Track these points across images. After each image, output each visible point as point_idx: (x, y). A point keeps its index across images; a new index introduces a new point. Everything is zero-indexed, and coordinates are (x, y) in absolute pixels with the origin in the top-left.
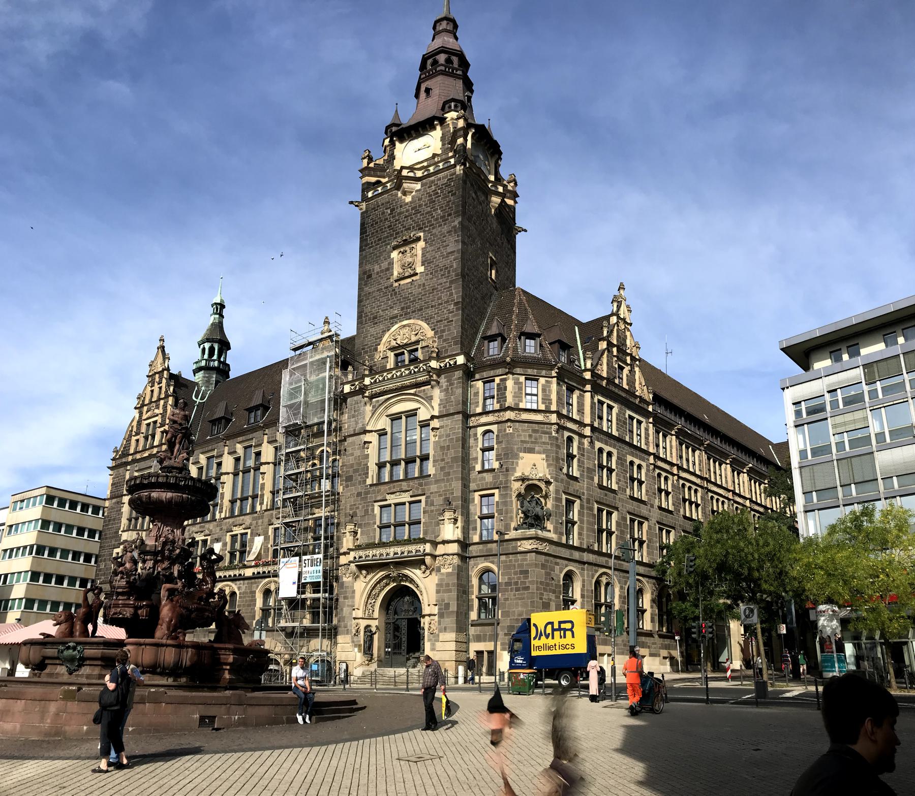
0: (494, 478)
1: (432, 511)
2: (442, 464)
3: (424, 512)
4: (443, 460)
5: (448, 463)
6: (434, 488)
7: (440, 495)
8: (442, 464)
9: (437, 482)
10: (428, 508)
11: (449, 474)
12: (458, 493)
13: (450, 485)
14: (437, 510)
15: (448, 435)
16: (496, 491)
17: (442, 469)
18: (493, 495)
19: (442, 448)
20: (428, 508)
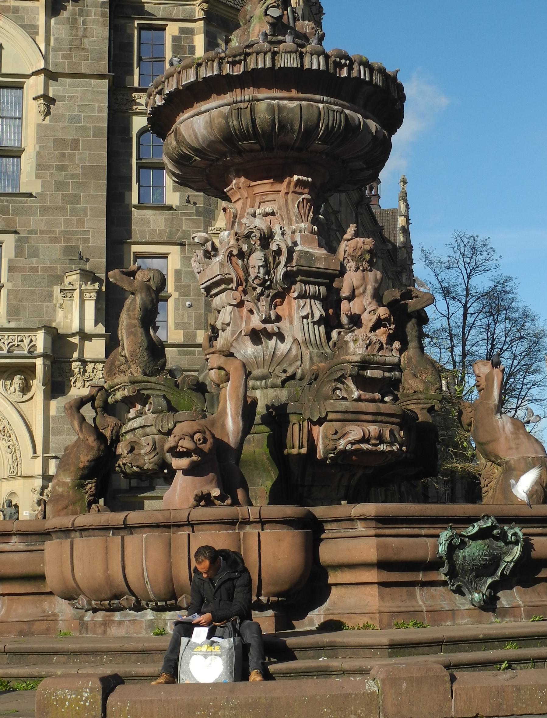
0: (170, 222)
1: (34, 270)
2: (61, 176)
3: (11, 269)
4: (62, 168)
5: (73, 176)
6: (37, 222)
7: (55, 240)
8: (61, 176)
9: (45, 210)
10: (21, 262)
11: (76, 199)
12: (99, 240)
13: (81, 222)
14: (45, 269)
15: (72, 119)
16: (174, 251)
17: (59, 186)
18: (164, 256)
19: (60, 143)
20: (21, 262)
